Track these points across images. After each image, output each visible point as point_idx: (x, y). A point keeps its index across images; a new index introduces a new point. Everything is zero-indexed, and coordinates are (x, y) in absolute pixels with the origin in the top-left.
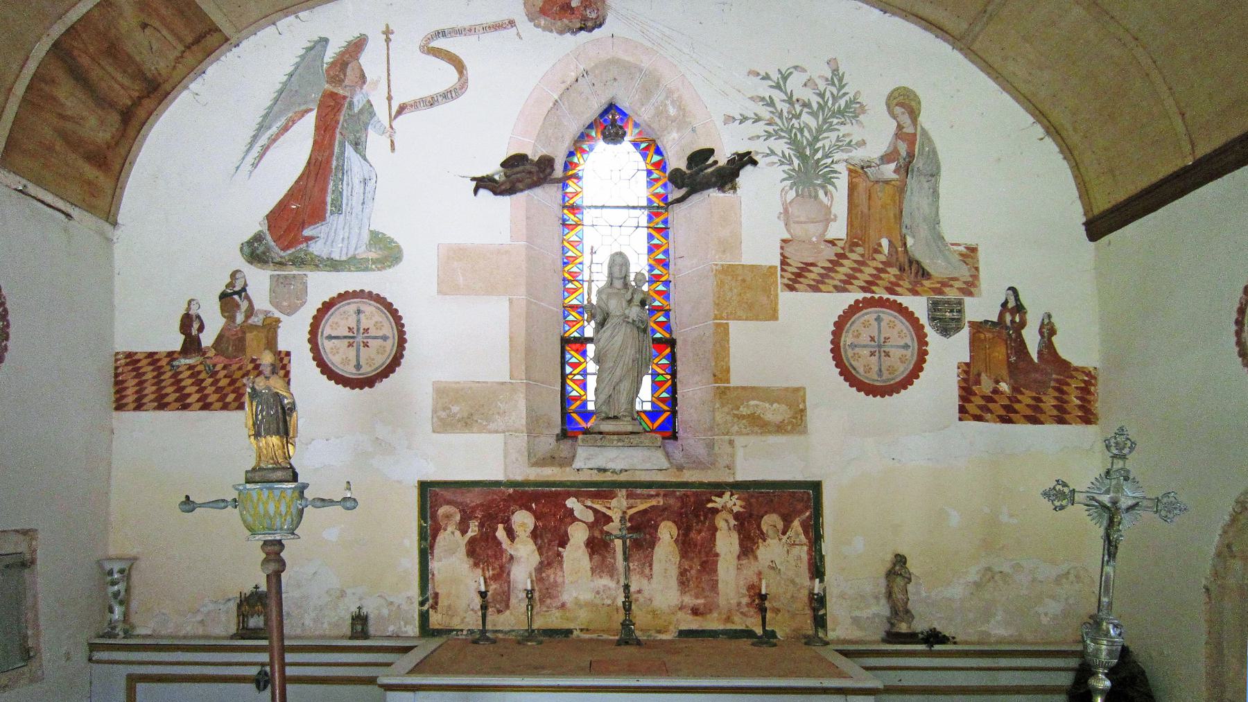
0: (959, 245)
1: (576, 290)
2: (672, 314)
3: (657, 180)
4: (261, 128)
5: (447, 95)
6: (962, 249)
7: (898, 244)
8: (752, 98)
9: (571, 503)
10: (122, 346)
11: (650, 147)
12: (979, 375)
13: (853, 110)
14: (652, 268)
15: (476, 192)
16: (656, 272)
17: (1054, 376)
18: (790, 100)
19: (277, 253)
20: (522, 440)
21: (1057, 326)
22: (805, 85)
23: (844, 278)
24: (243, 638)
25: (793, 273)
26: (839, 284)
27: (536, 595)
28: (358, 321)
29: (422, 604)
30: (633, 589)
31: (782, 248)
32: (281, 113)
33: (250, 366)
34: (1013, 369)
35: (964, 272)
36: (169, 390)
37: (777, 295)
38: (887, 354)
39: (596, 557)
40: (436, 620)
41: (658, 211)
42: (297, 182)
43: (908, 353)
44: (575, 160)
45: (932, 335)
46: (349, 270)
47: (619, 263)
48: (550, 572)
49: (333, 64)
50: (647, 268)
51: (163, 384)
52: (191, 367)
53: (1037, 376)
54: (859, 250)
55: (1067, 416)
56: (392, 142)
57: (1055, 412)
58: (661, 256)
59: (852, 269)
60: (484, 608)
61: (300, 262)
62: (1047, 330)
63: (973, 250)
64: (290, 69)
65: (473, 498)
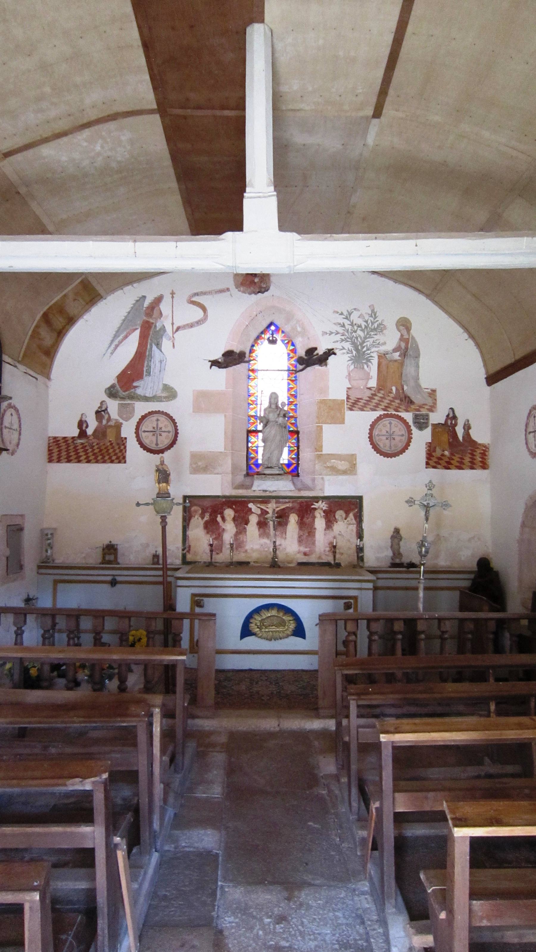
0: (427, 389)
1: (254, 408)
2: (298, 419)
3: (292, 358)
4: (116, 336)
5: (199, 323)
6: (429, 391)
7: (400, 389)
8: (335, 324)
9: (251, 505)
10: (52, 434)
11: (290, 342)
12: (435, 448)
13: (380, 328)
14: (289, 398)
15: (211, 367)
16: (291, 400)
17: (470, 448)
18: (352, 324)
19: (122, 393)
20: (229, 477)
21: (472, 426)
22: (359, 317)
23: (375, 405)
24: (103, 564)
25: (352, 403)
26: (372, 407)
27: (234, 546)
28: (157, 425)
29: (183, 550)
30: (277, 543)
31: (347, 391)
32: (125, 329)
33: (109, 444)
34: (451, 445)
35: (430, 401)
36: (72, 454)
37: (344, 412)
38: (394, 439)
39: (261, 530)
40: (189, 557)
41: (293, 372)
42: (131, 361)
43: (403, 438)
44: (254, 348)
45: (414, 430)
46: (154, 402)
47: (274, 397)
48: (241, 536)
49: (148, 308)
50: (287, 398)
51: (70, 451)
52: (82, 444)
53: (462, 448)
54: (382, 392)
55: (474, 466)
56: (173, 344)
57: (470, 464)
58: (293, 393)
59: (379, 400)
60: (211, 551)
61: (134, 397)
62: (467, 427)
63: (434, 391)
64: (128, 310)
65: (207, 503)
